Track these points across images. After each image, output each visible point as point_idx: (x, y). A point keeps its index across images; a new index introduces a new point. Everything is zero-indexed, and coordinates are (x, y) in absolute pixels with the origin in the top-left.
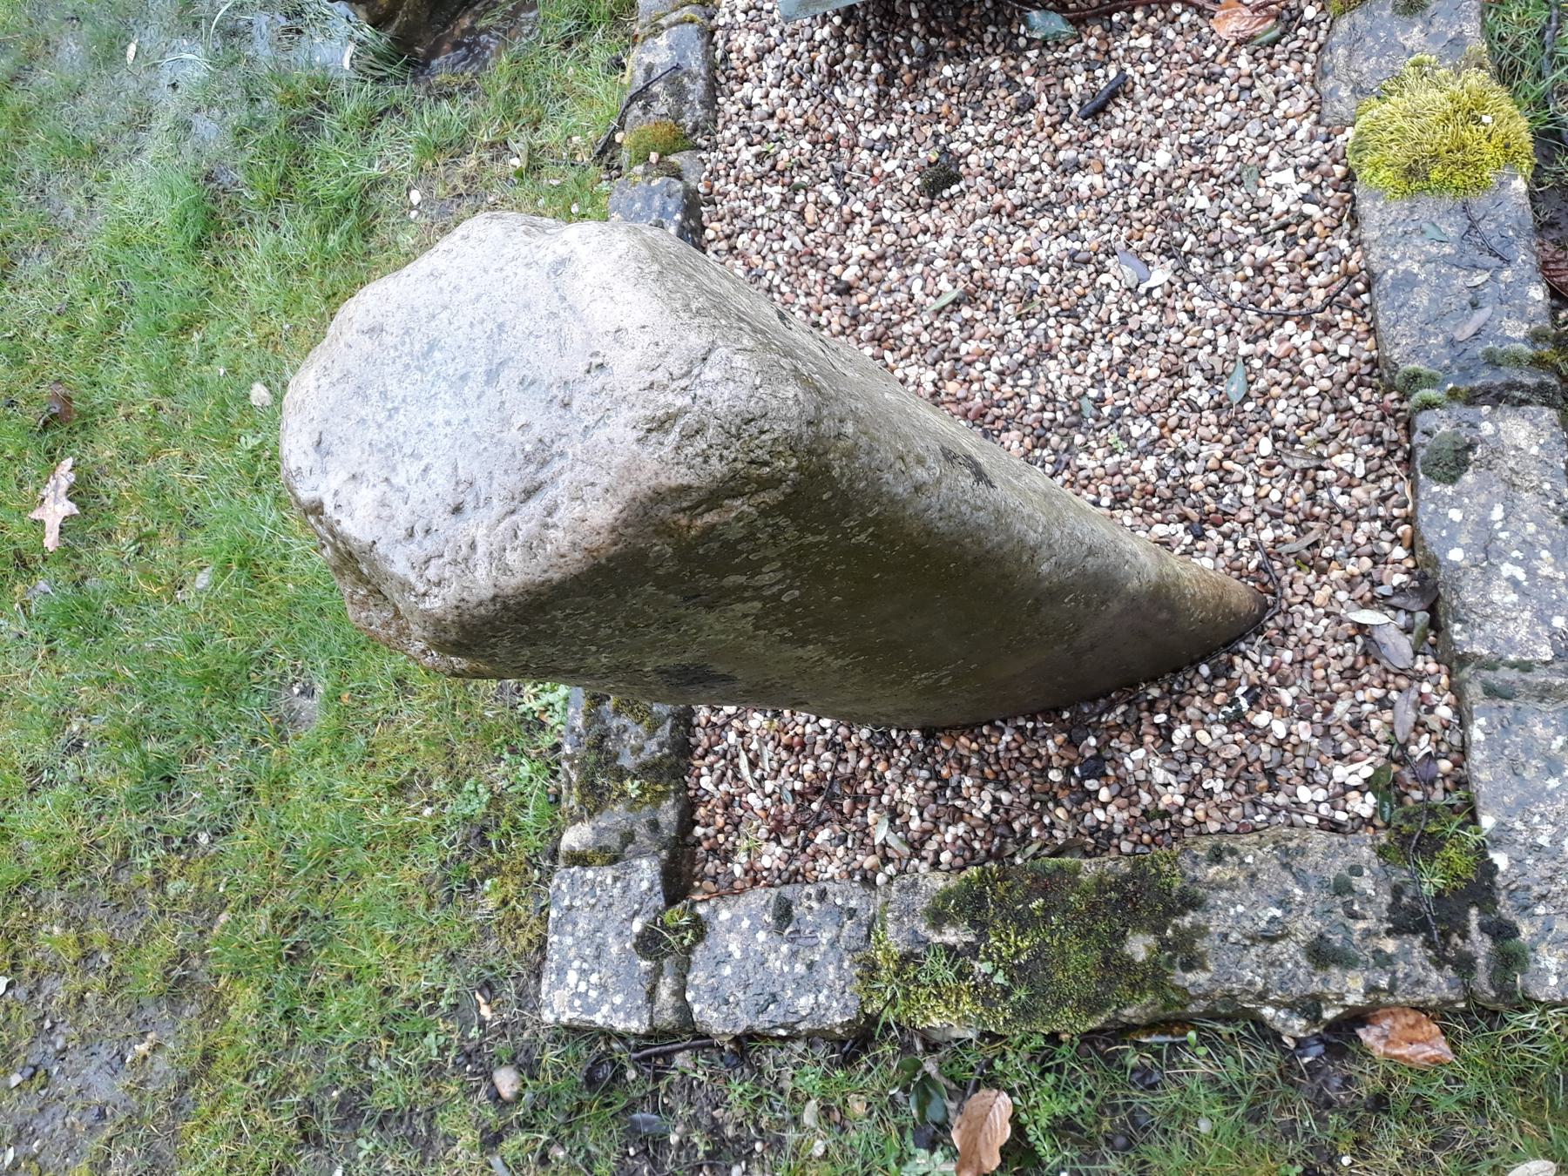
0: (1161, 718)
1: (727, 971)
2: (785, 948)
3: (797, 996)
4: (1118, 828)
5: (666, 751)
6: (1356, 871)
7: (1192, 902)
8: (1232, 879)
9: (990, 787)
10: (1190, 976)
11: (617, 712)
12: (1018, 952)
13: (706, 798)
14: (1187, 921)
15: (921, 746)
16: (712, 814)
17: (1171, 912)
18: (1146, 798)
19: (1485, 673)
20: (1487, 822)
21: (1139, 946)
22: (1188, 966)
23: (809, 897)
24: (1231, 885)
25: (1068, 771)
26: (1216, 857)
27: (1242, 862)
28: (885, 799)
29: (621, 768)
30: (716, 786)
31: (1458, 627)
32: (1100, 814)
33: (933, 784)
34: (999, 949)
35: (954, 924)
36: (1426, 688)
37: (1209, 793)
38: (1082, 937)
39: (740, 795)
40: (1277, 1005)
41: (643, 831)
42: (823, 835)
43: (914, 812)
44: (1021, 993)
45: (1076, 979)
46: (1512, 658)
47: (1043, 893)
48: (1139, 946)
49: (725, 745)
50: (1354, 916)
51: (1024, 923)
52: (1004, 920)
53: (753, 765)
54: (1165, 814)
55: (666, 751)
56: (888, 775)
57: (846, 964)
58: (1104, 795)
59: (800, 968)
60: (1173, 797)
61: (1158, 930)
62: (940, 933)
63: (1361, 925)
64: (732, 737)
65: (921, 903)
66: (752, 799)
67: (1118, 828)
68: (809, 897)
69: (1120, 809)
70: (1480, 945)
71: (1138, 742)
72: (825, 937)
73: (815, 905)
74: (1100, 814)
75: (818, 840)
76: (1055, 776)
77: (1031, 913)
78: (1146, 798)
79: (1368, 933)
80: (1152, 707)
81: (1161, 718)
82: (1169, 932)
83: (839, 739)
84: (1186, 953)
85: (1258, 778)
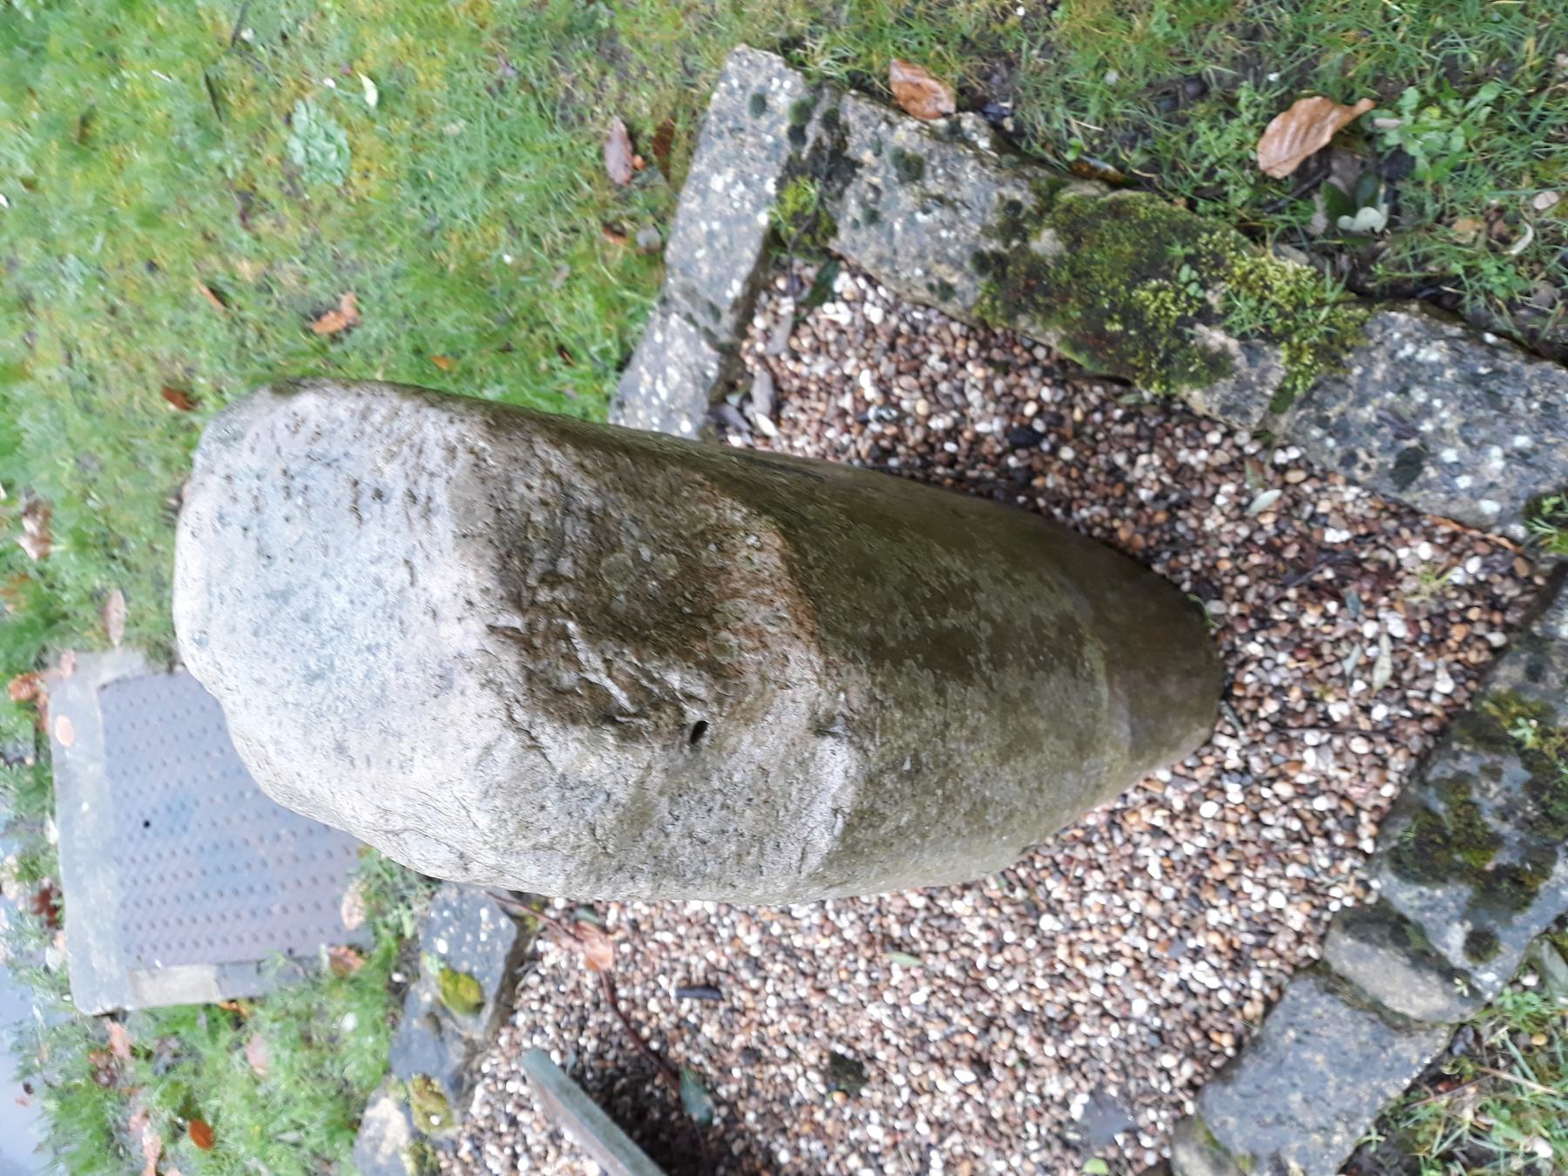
0: (950, 447)
1: (1522, 441)
2: (1427, 427)
3: (1439, 368)
4: (1036, 372)
5: (1456, 746)
6: (856, 224)
7: (983, 262)
8: (939, 262)
9: (1129, 479)
10: (1018, 196)
11: (1496, 841)
12: (1156, 291)
13: (1457, 667)
14: (994, 245)
15: (1166, 555)
16: (1465, 643)
17: (999, 258)
18: (999, 385)
19: (712, 328)
20: (763, 219)
21: (1045, 243)
22: (1015, 206)
23: (1366, 468)
24: (942, 257)
25: (1054, 450)
26: (946, 291)
27: (927, 273)
28: (1243, 531)
29: (1529, 766)
30: (1432, 673)
31: (710, 373)
32: (1046, 394)
33: (1181, 514)
34: (1175, 302)
35: (1205, 348)
36: (760, 347)
37: (945, 358)
38: (1087, 274)
39: (1414, 643)
40: (973, 145)
41: (1551, 675)
42: (1334, 536)
43: (1220, 500)
44: (1178, 250)
45: (1116, 240)
46: (692, 329)
47: (1101, 334)
48: (1045, 243)
49: (1394, 710)
50: (876, 189)
51: (1131, 314)
52: (1155, 327)
53: (1370, 665)
54: (989, 362)
55: (1456, 746)
56: (1224, 552)
57: (1357, 371)
58: (1030, 409)
59: (1419, 395)
60: (975, 372)
61: (1023, 250)
62: (1224, 346)
63: (876, 180)
64: (1380, 712)
65: (1225, 385)
66: (1398, 628)
67: (1036, 372)
68: (1366, 468)
69: (1025, 389)
70: (813, 130)
71: (979, 438)
72: (1368, 413)
73: (1362, 455)
74: (1046, 394)
75: (1345, 535)
76: (1067, 453)
77: (1124, 321)
78: (999, 385)
79: (874, 171)
80: (952, 461)
81: (950, 447)
82: (1015, 243)
83: (1252, 623)
84: (1014, 223)
85: (904, 348)
